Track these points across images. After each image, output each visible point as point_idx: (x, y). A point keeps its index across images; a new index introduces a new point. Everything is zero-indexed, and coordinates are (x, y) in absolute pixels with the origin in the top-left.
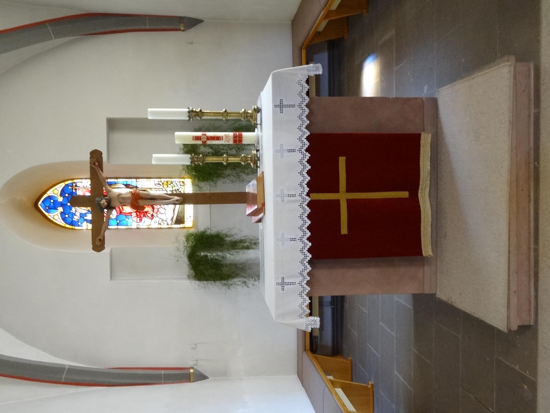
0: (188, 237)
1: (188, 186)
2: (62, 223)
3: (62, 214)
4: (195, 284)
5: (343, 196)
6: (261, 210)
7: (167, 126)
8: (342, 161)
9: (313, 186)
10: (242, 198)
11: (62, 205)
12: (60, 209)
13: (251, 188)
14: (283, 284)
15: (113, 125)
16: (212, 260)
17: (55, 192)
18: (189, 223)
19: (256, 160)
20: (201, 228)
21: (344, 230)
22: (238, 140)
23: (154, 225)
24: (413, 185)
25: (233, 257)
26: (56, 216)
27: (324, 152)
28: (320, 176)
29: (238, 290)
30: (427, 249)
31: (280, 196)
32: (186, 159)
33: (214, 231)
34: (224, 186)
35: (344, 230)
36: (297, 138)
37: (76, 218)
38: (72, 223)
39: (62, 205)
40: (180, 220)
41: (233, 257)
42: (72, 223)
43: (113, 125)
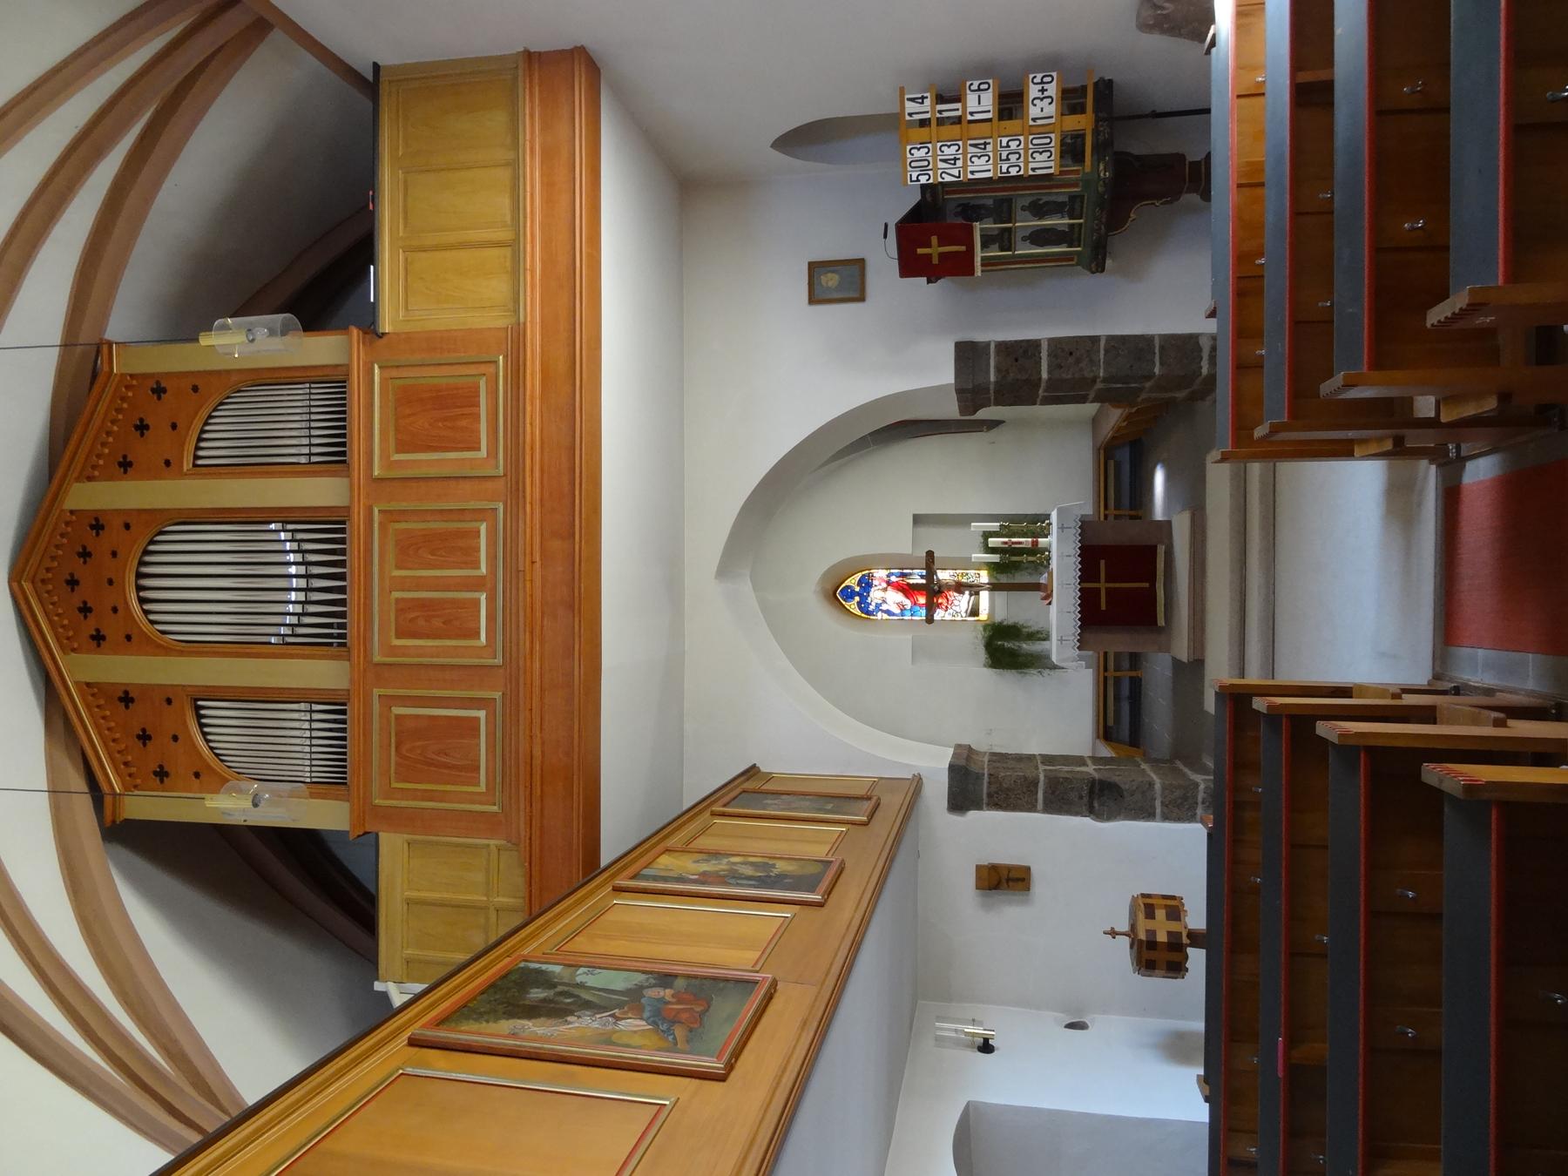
0: (986, 627)
1: (984, 577)
2: (858, 612)
3: (859, 604)
4: (990, 673)
5: (1103, 586)
6: (1049, 596)
7: (964, 520)
8: (1102, 563)
9: (1082, 579)
10: (1036, 587)
11: (858, 594)
12: (857, 598)
13: (1043, 580)
14: (1061, 640)
15: (918, 520)
16: (1007, 648)
17: (852, 582)
18: (983, 616)
19: (1049, 559)
20: (998, 619)
21: (1103, 607)
22: (1035, 544)
23: (948, 617)
24: (1152, 579)
25: (1027, 647)
26: (852, 606)
27: (1091, 556)
28: (1088, 571)
29: (1034, 678)
30: (1161, 622)
31: (1061, 584)
32: (995, 558)
33: (1011, 622)
34: (1022, 578)
35: (1103, 607)
36: (1073, 548)
37: (872, 608)
38: (868, 613)
39: (858, 594)
40: (974, 612)
41: (1027, 647)
42: (868, 613)
43: (918, 520)
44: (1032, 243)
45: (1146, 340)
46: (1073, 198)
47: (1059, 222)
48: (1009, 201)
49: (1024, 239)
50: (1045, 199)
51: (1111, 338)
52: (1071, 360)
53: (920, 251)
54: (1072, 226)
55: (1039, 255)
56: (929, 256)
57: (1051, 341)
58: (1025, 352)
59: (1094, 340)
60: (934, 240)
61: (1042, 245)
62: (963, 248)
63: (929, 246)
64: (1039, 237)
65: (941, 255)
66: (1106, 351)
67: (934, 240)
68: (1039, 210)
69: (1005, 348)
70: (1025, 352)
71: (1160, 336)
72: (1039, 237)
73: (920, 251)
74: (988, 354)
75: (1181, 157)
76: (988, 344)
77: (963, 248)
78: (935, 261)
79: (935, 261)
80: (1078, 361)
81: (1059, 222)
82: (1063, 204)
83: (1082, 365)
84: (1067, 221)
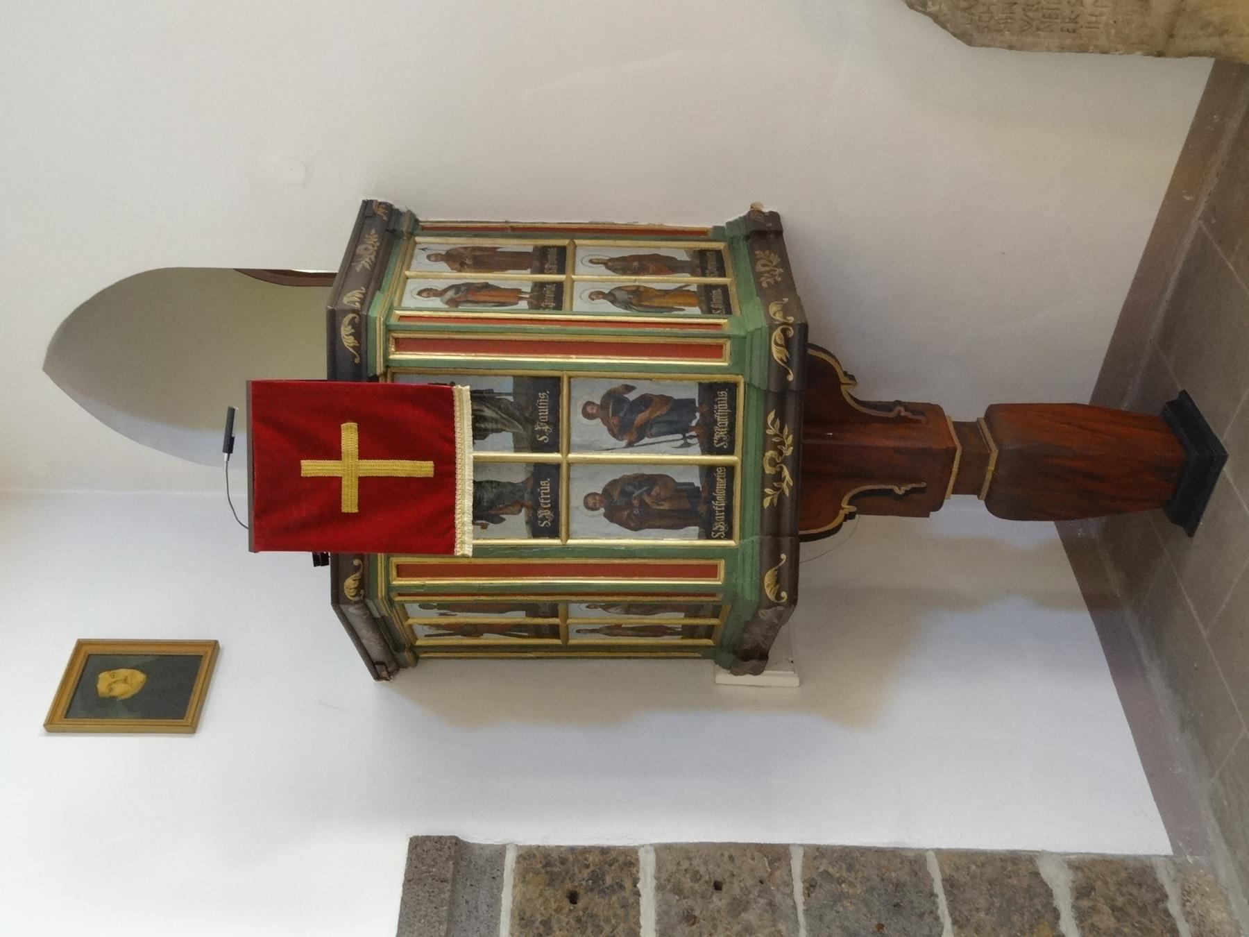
44: (612, 516)
45: (913, 861)
46: (709, 390)
47: (676, 457)
48: (551, 385)
49: (591, 503)
50: (643, 388)
51: (816, 853)
52: (719, 901)
53: (311, 468)
54: (708, 471)
55: (629, 552)
56: (333, 484)
57: (663, 851)
58: (597, 878)
59: (777, 855)
60: (349, 436)
61: (635, 524)
62: (424, 468)
63: (333, 452)
64: (630, 500)
65: (365, 483)
66: (810, 886)
67: (349, 436)
68: (628, 415)
69: (546, 866)
70: (597, 878)
71: (945, 856)
72: (630, 500)
73: (311, 468)
74: (497, 879)
75: (935, 411)
76: (500, 851)
77: (424, 468)
78: (350, 502)
79: (350, 502)
80: (738, 906)
81: (676, 457)
82: (685, 406)
83: (750, 916)
84: (695, 456)
